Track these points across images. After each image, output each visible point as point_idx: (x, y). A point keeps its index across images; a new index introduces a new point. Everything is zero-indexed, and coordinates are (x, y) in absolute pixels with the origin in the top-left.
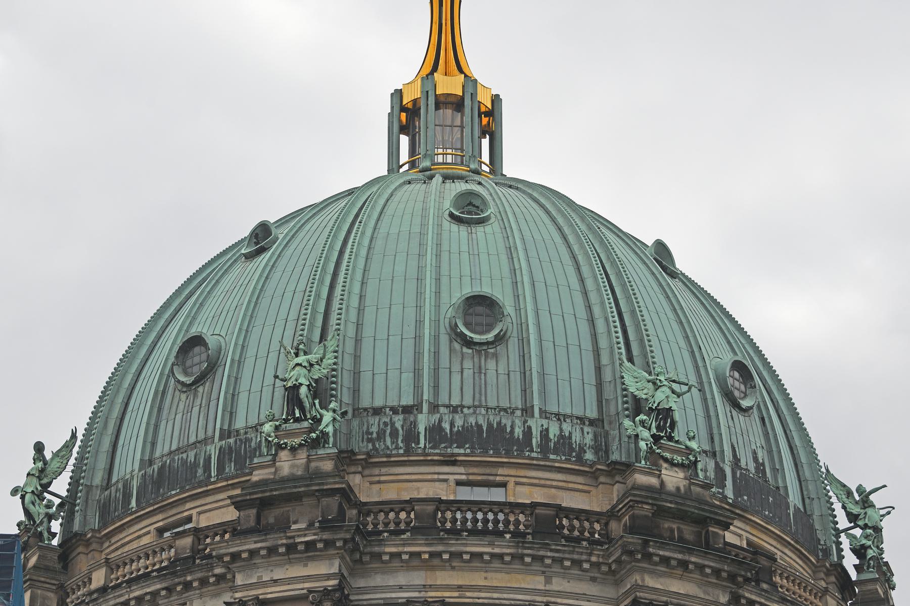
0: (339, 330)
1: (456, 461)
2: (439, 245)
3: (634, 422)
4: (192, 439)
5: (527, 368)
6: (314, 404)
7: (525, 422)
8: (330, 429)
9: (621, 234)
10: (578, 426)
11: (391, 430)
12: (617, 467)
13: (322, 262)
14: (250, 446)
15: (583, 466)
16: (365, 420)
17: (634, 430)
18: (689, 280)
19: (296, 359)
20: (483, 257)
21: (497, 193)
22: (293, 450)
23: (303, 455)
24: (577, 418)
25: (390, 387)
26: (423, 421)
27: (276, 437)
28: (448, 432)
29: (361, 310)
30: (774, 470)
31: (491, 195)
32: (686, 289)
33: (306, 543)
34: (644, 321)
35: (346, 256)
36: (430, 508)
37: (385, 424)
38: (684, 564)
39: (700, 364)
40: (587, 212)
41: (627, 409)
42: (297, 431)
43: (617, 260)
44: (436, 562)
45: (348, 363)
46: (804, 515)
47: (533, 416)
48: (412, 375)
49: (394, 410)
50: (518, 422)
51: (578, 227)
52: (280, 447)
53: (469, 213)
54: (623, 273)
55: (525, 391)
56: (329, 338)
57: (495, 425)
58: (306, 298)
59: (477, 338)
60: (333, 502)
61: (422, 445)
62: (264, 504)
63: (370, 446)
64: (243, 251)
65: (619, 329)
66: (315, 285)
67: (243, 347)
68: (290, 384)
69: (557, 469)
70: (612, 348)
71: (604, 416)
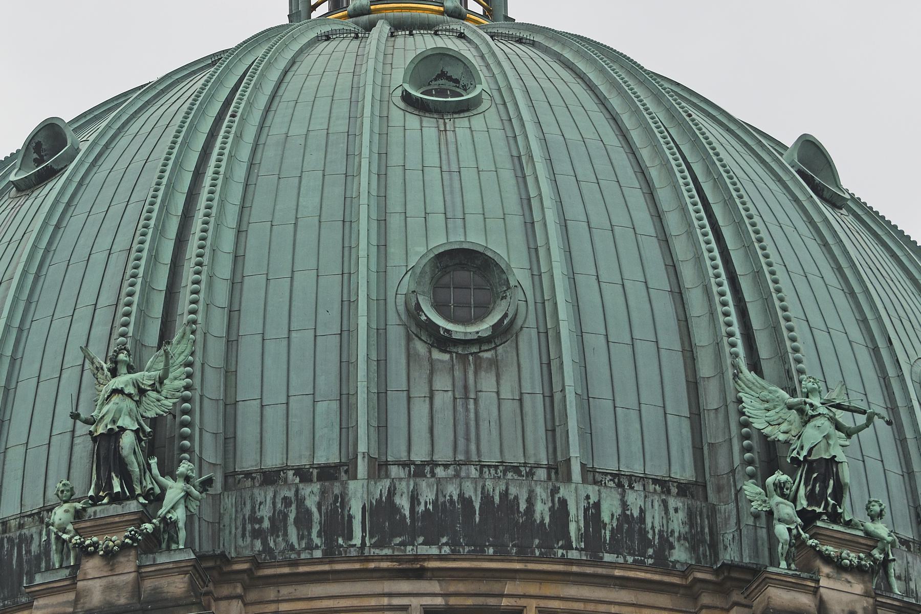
0: (194, 322)
1: (423, 570)
3: (764, 487)
5: (557, 388)
6: (149, 465)
7: (555, 491)
9: (732, 126)
10: (656, 497)
11: (297, 513)
12: (734, 575)
13: (160, 194)
14: (29, 552)
15: (668, 574)
16: (247, 494)
17: (765, 502)
18: (869, 211)
19: (113, 380)
21: (493, 54)
22: (110, 556)
23: (128, 566)
24: (655, 481)
25: (294, 429)
27: (77, 532)
28: (407, 513)
31: (482, 57)
32: (863, 229)
34: (778, 291)
35: (207, 181)
37: (287, 501)
39: (891, 372)
40: (666, 85)
41: (750, 462)
42: (117, 519)
43: (725, 175)
45: (213, 385)
47: (568, 479)
48: (335, 405)
49: (303, 475)
50: (541, 492)
51: (650, 114)
52: (84, 552)
53: (441, 92)
54: (738, 201)
55: (554, 431)
56: (174, 341)
57: (497, 499)
58: (131, 264)
59: (458, 330)
61: (357, 541)
63: (258, 545)
64: (12, 177)
65: (731, 308)
66: (148, 238)
68: (101, 430)
69: (618, 582)
70: (718, 345)
71: (707, 476)
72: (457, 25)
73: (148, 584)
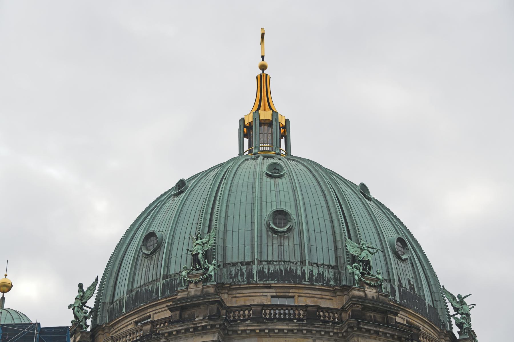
0: (216, 227)
1: (271, 286)
2: (261, 188)
3: (352, 267)
4: (150, 280)
5: (303, 243)
6: (205, 261)
7: (302, 268)
8: (213, 273)
9: (344, 181)
10: (326, 269)
11: (241, 273)
12: (345, 288)
13: (208, 197)
14: (177, 282)
15: (329, 287)
16: (229, 268)
17: (352, 270)
19: (197, 241)
20: (282, 193)
21: (287, 163)
22: (196, 283)
23: (200, 285)
24: (326, 265)
25: (240, 253)
26: (255, 269)
27: (188, 277)
28: (267, 273)
29: (226, 218)
30: (418, 288)
31: (285, 164)
32: (376, 205)
33: (202, 326)
34: (355, 220)
35: (219, 194)
36: (259, 309)
37: (238, 270)
38: (377, 333)
39: (382, 239)
40: (329, 171)
41: (349, 261)
42: (198, 274)
43: (343, 192)
44: (262, 333)
46: (433, 309)
47: (305, 265)
48: (250, 247)
49: (242, 264)
50: (299, 268)
51: (325, 178)
52: (190, 282)
53: (275, 173)
54: (346, 199)
55: (302, 253)
56: (211, 232)
57: (288, 270)
58: (201, 214)
59: (279, 229)
60: (215, 307)
61: (255, 279)
62: (183, 309)
63: (231, 281)
64: (173, 193)
65: (344, 224)
66: (205, 207)
67: (173, 236)
68: (194, 253)
69: (317, 289)
70: (341, 233)
71: (338, 264)
72: (279, 157)
73: (205, 290)
